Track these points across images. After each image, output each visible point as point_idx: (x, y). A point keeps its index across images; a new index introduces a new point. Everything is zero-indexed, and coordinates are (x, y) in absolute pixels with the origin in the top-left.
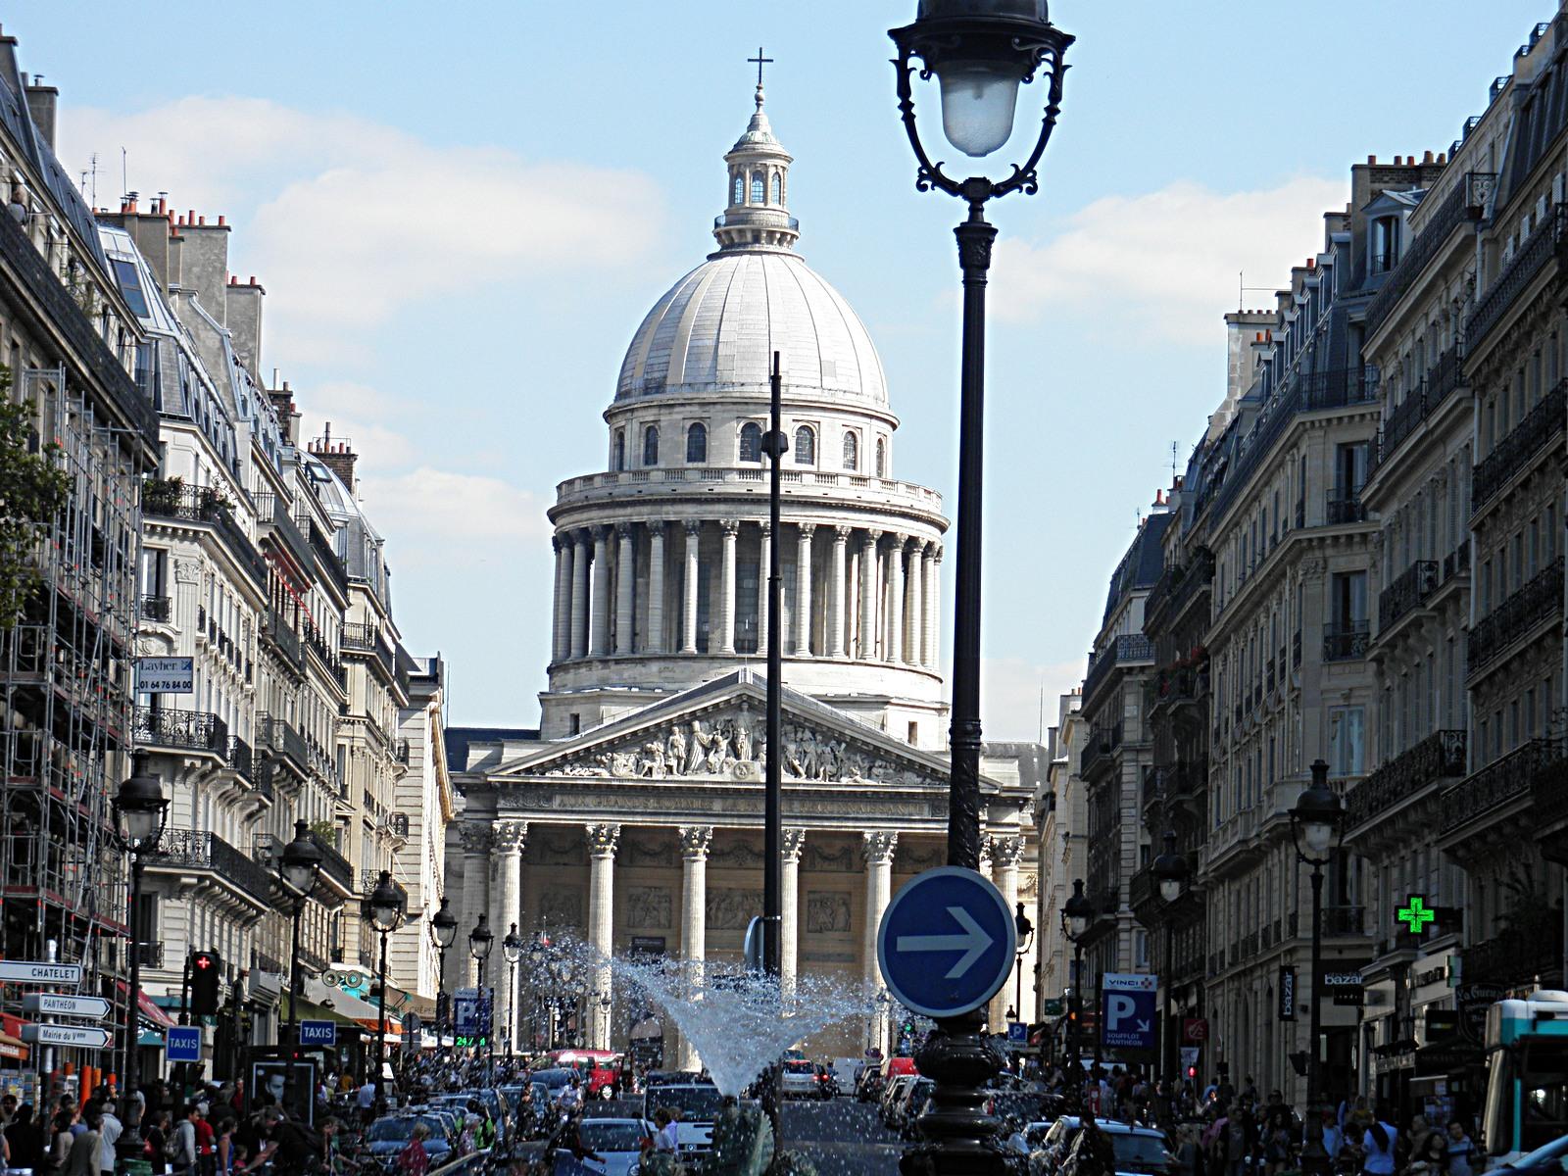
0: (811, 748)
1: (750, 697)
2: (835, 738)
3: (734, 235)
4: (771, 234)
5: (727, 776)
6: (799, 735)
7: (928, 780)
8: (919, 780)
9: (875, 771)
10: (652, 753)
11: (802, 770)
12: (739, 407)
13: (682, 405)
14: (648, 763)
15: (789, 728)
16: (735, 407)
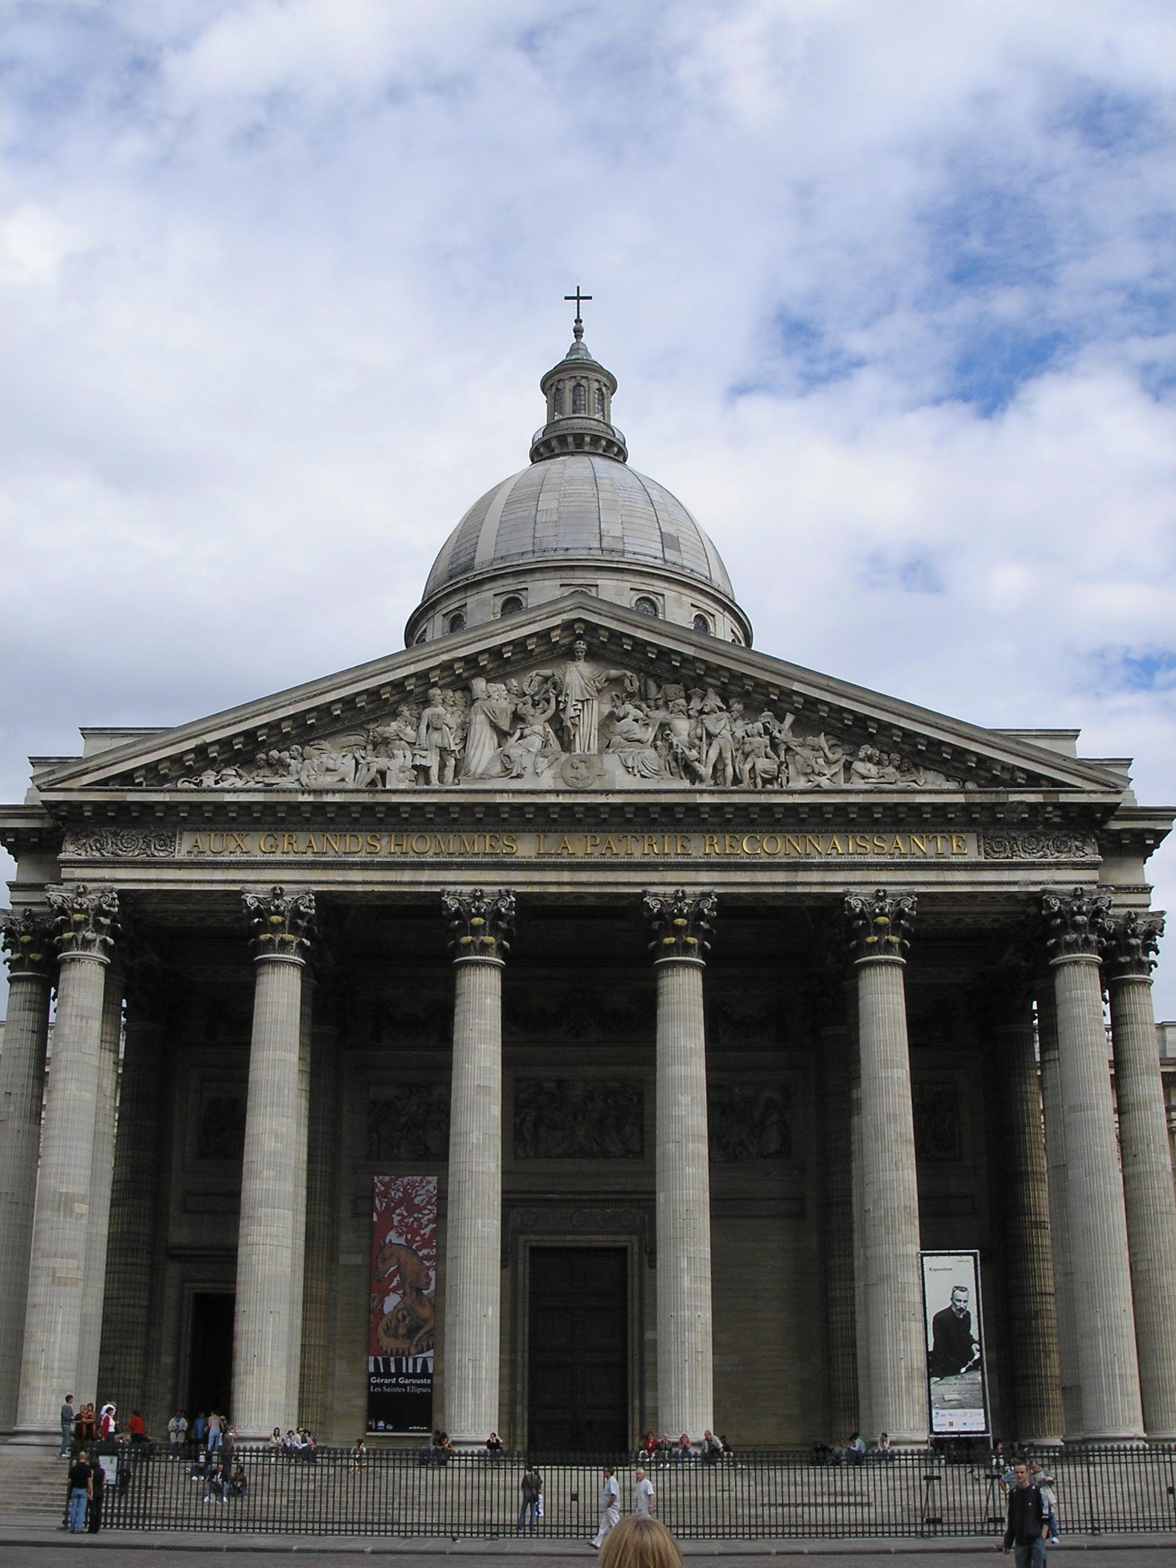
0: (720, 724)
1: (592, 628)
2: (771, 705)
3: (554, 443)
4: (596, 440)
5: (547, 781)
6: (696, 704)
7: (970, 786)
8: (952, 785)
9: (859, 766)
10: (386, 742)
11: (705, 770)
12: (564, 574)
13: (493, 579)
14: (381, 762)
15: (672, 689)
16: (558, 574)
